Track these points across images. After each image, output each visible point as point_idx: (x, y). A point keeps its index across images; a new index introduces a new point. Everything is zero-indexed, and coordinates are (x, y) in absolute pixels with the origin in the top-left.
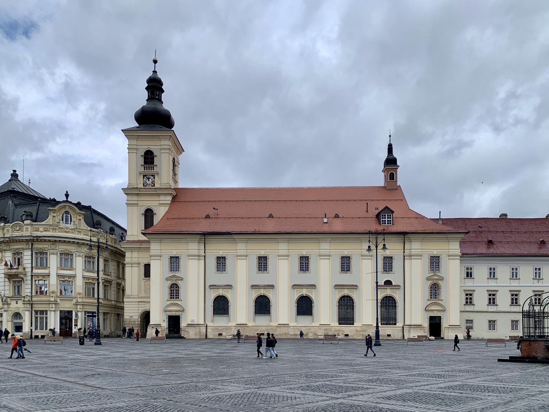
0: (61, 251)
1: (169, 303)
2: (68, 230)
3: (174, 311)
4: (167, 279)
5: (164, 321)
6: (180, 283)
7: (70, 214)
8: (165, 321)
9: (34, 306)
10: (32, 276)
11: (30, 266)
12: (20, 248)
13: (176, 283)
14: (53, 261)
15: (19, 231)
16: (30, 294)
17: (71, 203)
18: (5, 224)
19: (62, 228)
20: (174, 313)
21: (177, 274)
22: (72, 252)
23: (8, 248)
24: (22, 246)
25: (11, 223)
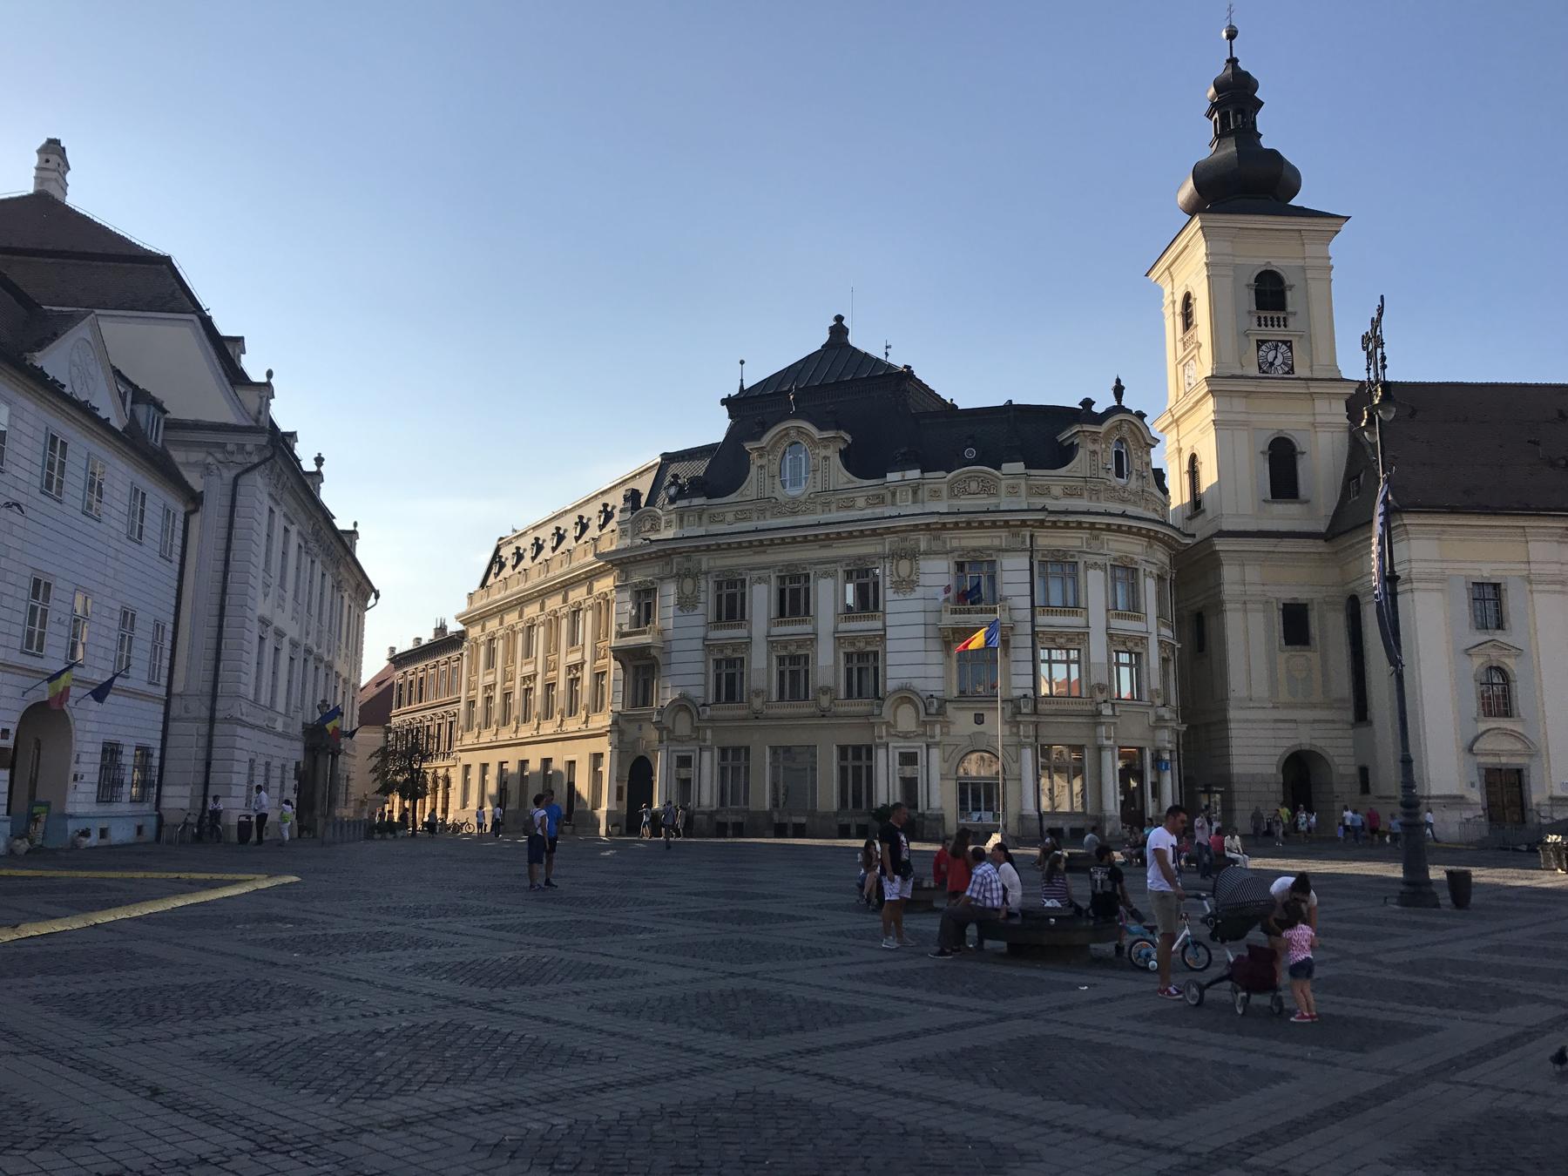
0: (1115, 560)
1: (1482, 727)
2: (1126, 495)
3: (1501, 749)
4: (1467, 652)
5: (1473, 785)
6: (1510, 663)
7: (1128, 446)
8: (1478, 784)
9: (1043, 731)
10: (1034, 634)
11: (1027, 602)
12: (988, 548)
13: (1501, 665)
14: (1095, 587)
15: (978, 496)
16: (1030, 693)
17: (1129, 411)
18: (922, 472)
19: (1114, 489)
20: (1504, 760)
21: (1499, 636)
22: (1136, 563)
23: (936, 546)
24: (996, 542)
25: (949, 472)
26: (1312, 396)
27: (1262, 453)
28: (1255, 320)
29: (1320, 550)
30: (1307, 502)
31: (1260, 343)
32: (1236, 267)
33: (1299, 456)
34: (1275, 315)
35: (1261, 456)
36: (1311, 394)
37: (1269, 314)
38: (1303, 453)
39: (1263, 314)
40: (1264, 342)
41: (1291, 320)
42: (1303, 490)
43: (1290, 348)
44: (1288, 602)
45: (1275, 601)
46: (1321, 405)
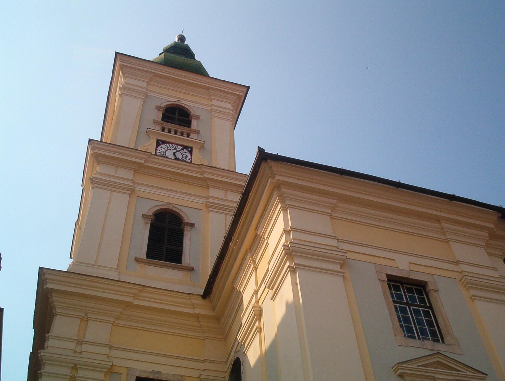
26: (206, 183)
27: (144, 216)
28: (158, 128)
29: (197, 311)
30: (191, 269)
31: (159, 143)
32: (147, 96)
33: (186, 228)
34: (180, 129)
35: (141, 221)
36: (206, 180)
37: (173, 127)
38: (192, 225)
39: (168, 125)
40: (164, 142)
41: (193, 136)
42: (187, 258)
43: (191, 152)
44: (144, 375)
45: (124, 372)
46: (215, 193)
